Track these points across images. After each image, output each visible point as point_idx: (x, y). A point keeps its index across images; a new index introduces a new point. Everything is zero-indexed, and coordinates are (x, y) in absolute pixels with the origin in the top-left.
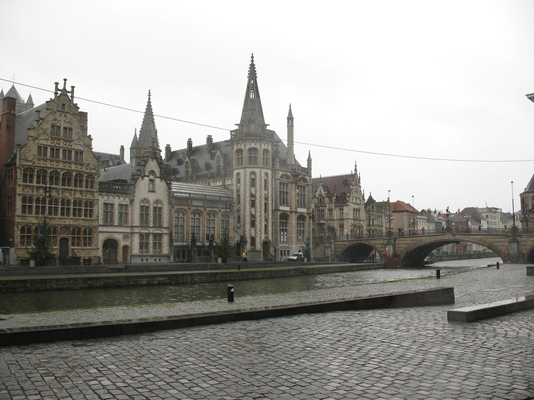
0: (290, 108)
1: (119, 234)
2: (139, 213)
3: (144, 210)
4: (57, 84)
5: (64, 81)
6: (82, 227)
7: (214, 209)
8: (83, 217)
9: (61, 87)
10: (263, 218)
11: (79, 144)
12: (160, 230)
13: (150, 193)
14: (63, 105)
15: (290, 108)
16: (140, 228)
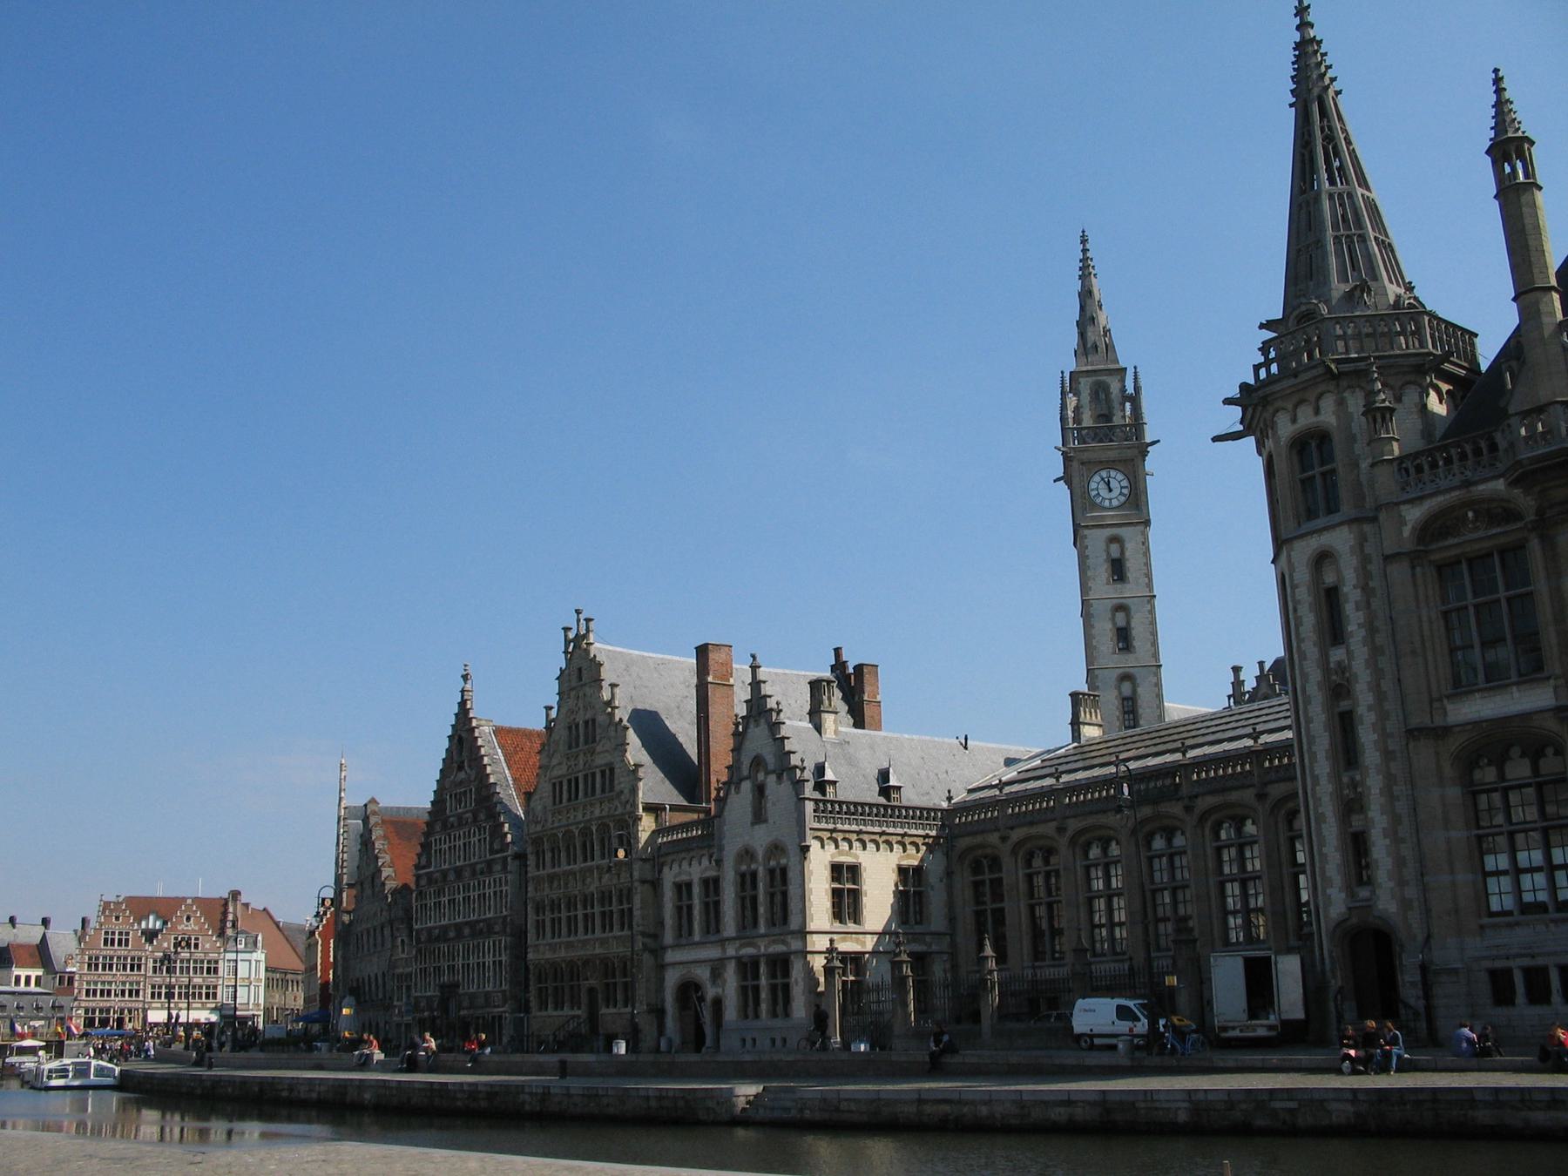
0: (1499, 91)
1: (703, 964)
2: (733, 895)
3: (747, 881)
4: (566, 630)
5: (576, 615)
6: (614, 957)
7: (1234, 796)
8: (598, 933)
9: (571, 635)
10: (1326, 799)
11: (605, 749)
12: (784, 942)
13: (756, 827)
14: (580, 670)
15: (1499, 91)
16: (738, 943)
